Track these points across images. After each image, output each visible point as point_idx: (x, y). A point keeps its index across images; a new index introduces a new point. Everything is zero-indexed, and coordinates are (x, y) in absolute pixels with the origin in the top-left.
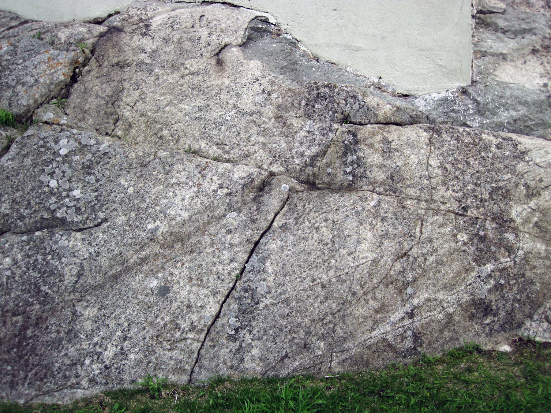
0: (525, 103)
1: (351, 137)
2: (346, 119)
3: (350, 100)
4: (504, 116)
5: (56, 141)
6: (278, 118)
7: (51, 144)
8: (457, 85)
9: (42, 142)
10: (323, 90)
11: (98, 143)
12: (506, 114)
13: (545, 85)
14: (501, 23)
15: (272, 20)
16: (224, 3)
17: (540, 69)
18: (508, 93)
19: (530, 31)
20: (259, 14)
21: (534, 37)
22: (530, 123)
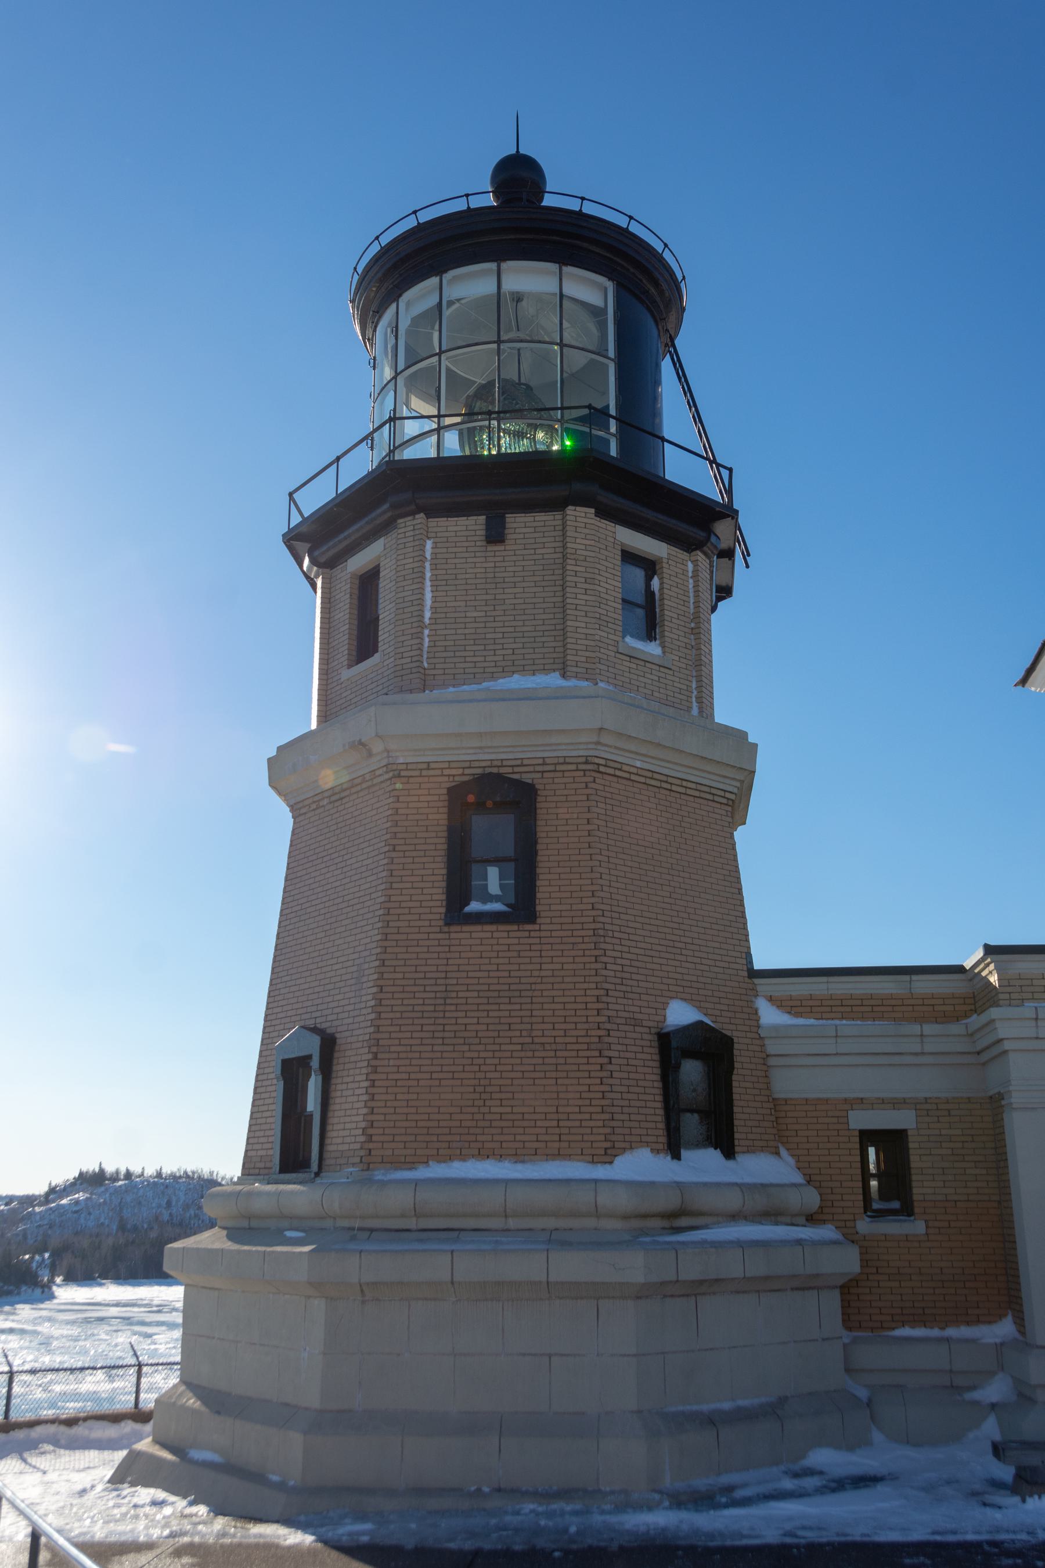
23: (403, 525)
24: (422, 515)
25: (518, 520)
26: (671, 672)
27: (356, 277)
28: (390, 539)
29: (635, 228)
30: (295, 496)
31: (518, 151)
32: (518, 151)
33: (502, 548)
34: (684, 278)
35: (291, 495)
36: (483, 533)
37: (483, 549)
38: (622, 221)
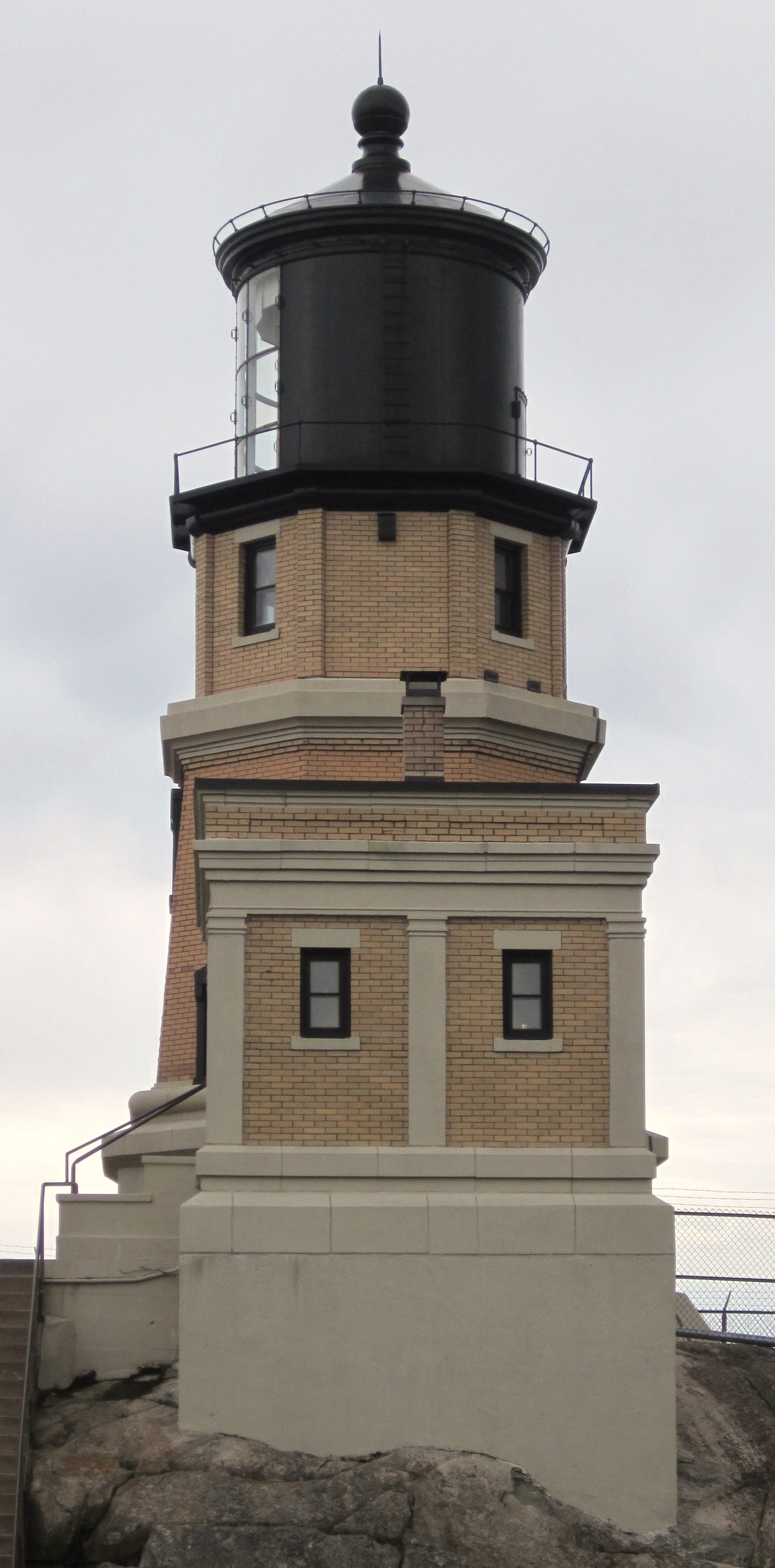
0: (716, 1539)
1: (609, 1561)
2: (601, 1549)
3: (603, 1536)
4: (703, 1548)
5: (433, 1557)
6: (561, 1547)
7: (430, 1559)
8: (667, 1525)
9: (423, 1558)
10: (584, 1529)
11: (459, 1560)
12: (703, 1547)
13: (730, 1526)
14: (692, 1473)
15: (524, 1472)
16: (482, 1454)
17: (725, 1513)
18: (704, 1532)
19: (714, 1480)
20: (515, 1466)
21: (718, 1486)
22: (720, 1554)
23: (303, 517)
24: (320, 510)
25: (408, 518)
26: (532, 653)
27: (229, 231)
28: (286, 523)
29: (511, 220)
30: (179, 457)
31: (380, 80)
32: (380, 80)
33: (393, 544)
34: (548, 242)
35: (176, 456)
36: (376, 528)
37: (376, 543)
38: (497, 214)
